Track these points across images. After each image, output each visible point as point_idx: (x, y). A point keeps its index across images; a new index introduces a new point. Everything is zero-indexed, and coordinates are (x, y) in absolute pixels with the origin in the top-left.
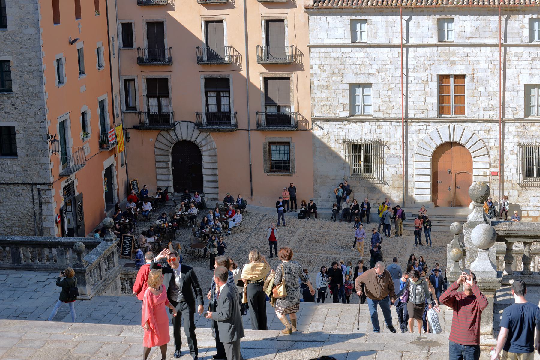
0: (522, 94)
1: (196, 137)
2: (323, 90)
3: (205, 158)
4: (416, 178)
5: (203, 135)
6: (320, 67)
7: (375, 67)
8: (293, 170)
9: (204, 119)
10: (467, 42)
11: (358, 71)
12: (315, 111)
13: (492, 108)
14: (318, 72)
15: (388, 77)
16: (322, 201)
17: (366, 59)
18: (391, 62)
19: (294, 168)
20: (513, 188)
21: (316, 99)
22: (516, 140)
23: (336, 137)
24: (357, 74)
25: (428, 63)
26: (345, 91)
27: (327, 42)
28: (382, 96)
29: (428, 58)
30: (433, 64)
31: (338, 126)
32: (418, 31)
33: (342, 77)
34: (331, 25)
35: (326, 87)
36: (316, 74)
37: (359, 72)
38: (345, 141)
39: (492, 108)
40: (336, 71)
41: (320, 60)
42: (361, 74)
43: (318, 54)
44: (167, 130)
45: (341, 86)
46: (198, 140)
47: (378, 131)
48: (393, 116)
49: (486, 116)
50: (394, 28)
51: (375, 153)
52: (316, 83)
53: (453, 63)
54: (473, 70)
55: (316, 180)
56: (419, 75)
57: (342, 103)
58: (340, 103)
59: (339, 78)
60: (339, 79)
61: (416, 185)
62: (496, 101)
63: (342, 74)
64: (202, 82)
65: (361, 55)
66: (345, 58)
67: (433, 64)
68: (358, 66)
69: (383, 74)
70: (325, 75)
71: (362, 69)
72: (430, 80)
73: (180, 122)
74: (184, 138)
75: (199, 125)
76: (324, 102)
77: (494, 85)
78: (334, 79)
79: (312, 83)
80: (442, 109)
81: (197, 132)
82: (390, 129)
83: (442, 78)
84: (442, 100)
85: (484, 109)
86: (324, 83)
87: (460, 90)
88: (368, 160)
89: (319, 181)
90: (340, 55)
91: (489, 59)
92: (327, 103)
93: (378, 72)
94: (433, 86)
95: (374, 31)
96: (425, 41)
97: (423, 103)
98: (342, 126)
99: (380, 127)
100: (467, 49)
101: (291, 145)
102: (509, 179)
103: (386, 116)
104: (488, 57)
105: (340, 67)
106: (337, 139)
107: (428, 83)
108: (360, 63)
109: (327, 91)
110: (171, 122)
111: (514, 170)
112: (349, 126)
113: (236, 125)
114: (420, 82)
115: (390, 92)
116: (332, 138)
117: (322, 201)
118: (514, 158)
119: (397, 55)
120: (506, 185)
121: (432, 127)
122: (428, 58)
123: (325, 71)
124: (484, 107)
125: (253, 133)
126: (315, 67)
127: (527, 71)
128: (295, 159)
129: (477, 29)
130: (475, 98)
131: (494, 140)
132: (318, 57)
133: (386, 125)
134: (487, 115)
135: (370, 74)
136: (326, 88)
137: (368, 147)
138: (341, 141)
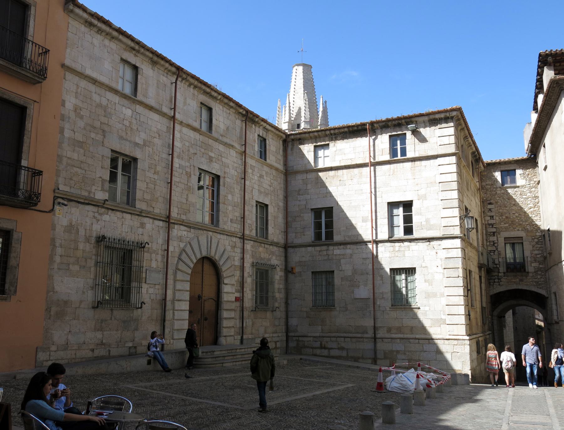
2: (77, 148)
6: (76, 109)
8: (12, 289)
11: (124, 134)
12: (61, 180)
14: (73, 115)
15: (155, 156)
16: (57, 350)
17: (134, 121)
18: (159, 136)
21: (65, 160)
23: (88, 231)
24: (121, 138)
25: (192, 151)
26: (105, 159)
27: (89, 72)
28: (148, 180)
30: (196, 154)
31: (91, 214)
32: (185, 108)
33: (104, 136)
35: (80, 144)
36: (69, 118)
37: (124, 137)
38: (101, 239)
40: (97, 124)
41: (76, 97)
42: (127, 140)
43: (75, 87)
47: (140, 230)
50: (164, 92)
52: (67, 133)
54: (225, 172)
55: (48, 310)
57: (100, 177)
58: (98, 176)
59: (99, 136)
60: (99, 137)
63: (104, 131)
66: (109, 109)
67: (196, 154)
68: (124, 128)
69: (150, 149)
71: (129, 133)
72: (192, 173)
76: (75, 169)
78: (93, 135)
79: (62, 131)
82: (153, 229)
89: (54, 309)
90: (104, 102)
91: (235, 165)
92: (79, 171)
95: (144, 86)
97: (185, 201)
98: (96, 215)
101: (15, 236)
102: (246, 306)
104: (234, 162)
105: (103, 120)
106: (87, 235)
107: (190, 176)
108: (127, 123)
109: (82, 151)
112: (106, 217)
114: (184, 172)
115: (156, 177)
116: (82, 232)
117: (57, 350)
123: (82, 117)
124: (231, 218)
126: (69, 105)
128: (18, 265)
130: (226, 206)
132: (74, 91)
133: (149, 224)
135: (136, 144)
136: (81, 147)
138: (93, 240)
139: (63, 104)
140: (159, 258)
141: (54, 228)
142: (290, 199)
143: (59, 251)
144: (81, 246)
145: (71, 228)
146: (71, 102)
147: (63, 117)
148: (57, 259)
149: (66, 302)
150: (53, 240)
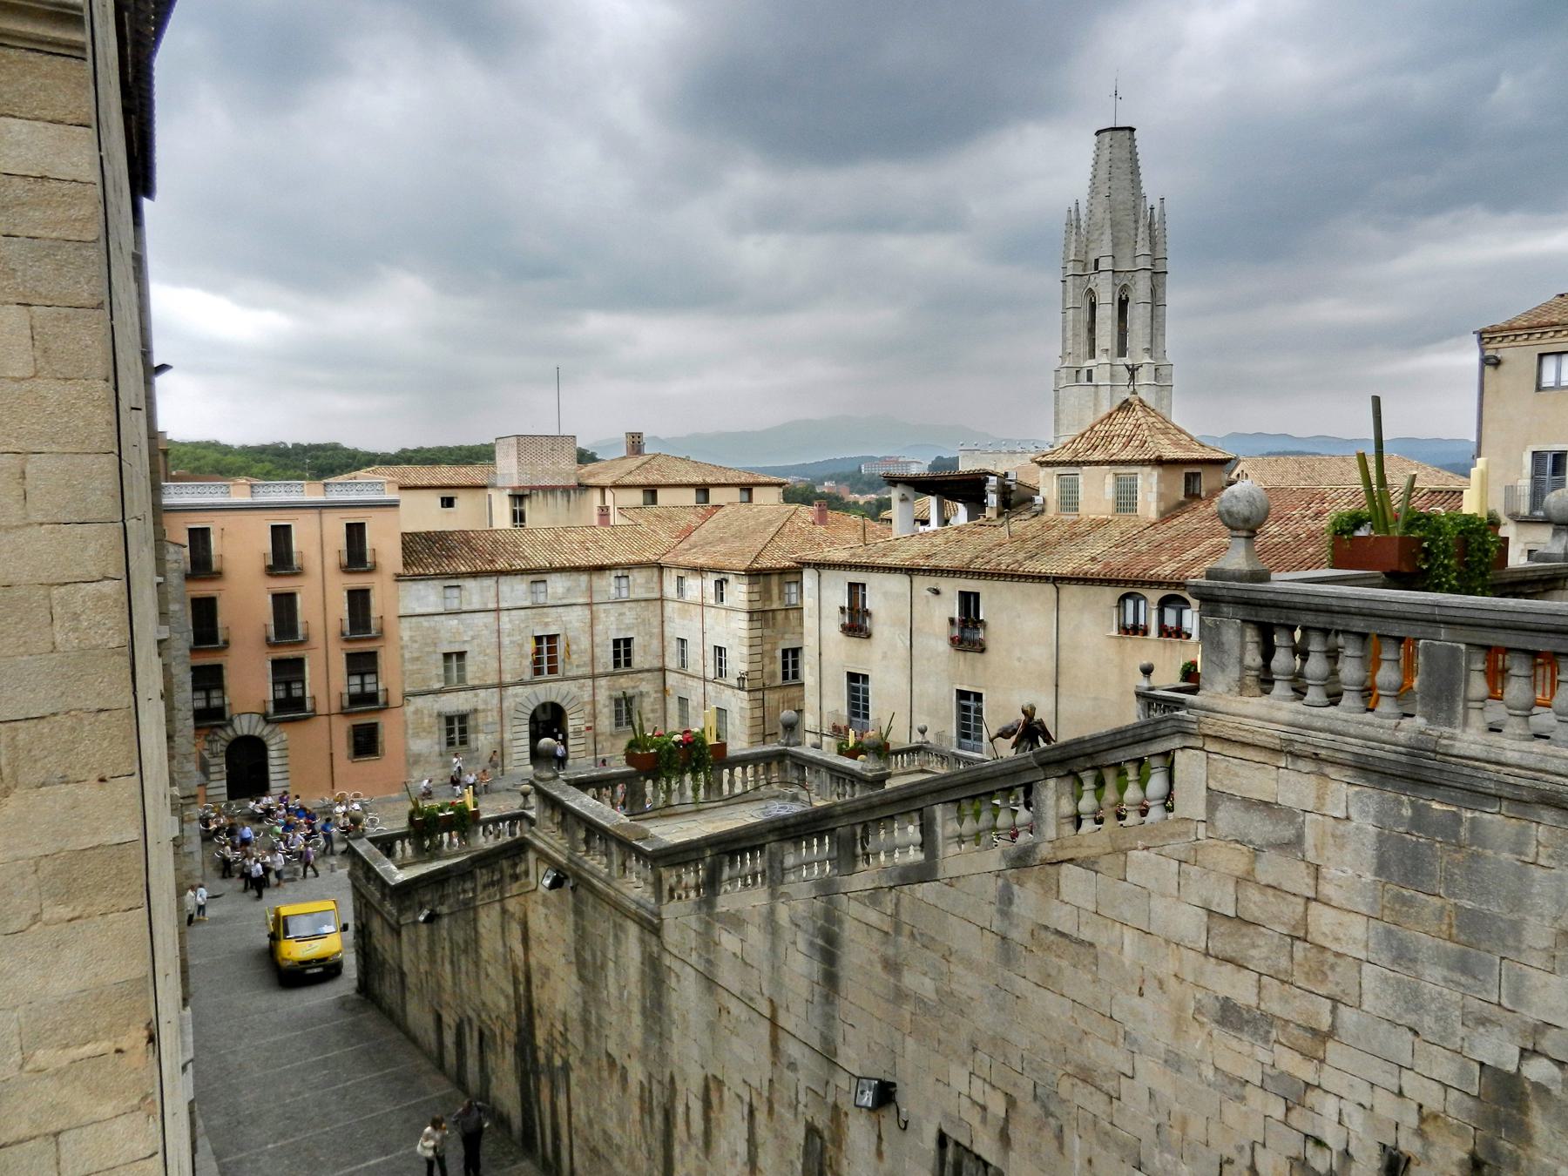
0: (611, 648)
1: (260, 730)
3: (273, 754)
4: (515, 743)
5: (269, 728)
6: (412, 639)
7: (471, 633)
9: (271, 708)
10: (560, 603)
13: (585, 665)
19: (383, 750)
20: (606, 740)
22: (607, 693)
25: (523, 625)
27: (419, 611)
29: (522, 621)
34: (422, 593)
35: (417, 659)
38: (439, 715)
39: (585, 665)
40: (429, 641)
44: (220, 727)
45: (434, 656)
46: (265, 733)
48: (489, 682)
49: (580, 673)
51: (471, 722)
52: (407, 655)
53: (547, 624)
55: (408, 761)
56: (515, 639)
61: (516, 750)
62: (587, 658)
64: (269, 665)
65: (456, 622)
70: (416, 645)
73: (239, 715)
74: (246, 732)
75: (266, 718)
77: (585, 643)
79: (402, 656)
80: (538, 672)
81: (262, 724)
83: (539, 639)
84: (538, 661)
85: (578, 666)
86: (416, 655)
87: (552, 650)
88: (463, 731)
90: (433, 624)
93: (473, 638)
94: (530, 646)
96: (520, 604)
99: (476, 695)
100: (560, 610)
103: (482, 683)
110: (227, 716)
111: (607, 723)
113: (314, 710)
116: (426, 712)
118: (606, 710)
119: (492, 620)
120: (598, 739)
121: (528, 690)
122: (522, 621)
125: (333, 718)
126: (406, 638)
127: (614, 627)
129: (569, 590)
131: (586, 696)
133: (482, 693)
134: (580, 672)
137: (463, 718)
139: (401, 638)
140: (495, 714)
141: (404, 714)
142: (666, 624)
143: (410, 726)
144: (426, 720)
145: (416, 712)
146: (406, 635)
147: (402, 648)
148: (410, 732)
149: (420, 755)
150: (405, 722)
